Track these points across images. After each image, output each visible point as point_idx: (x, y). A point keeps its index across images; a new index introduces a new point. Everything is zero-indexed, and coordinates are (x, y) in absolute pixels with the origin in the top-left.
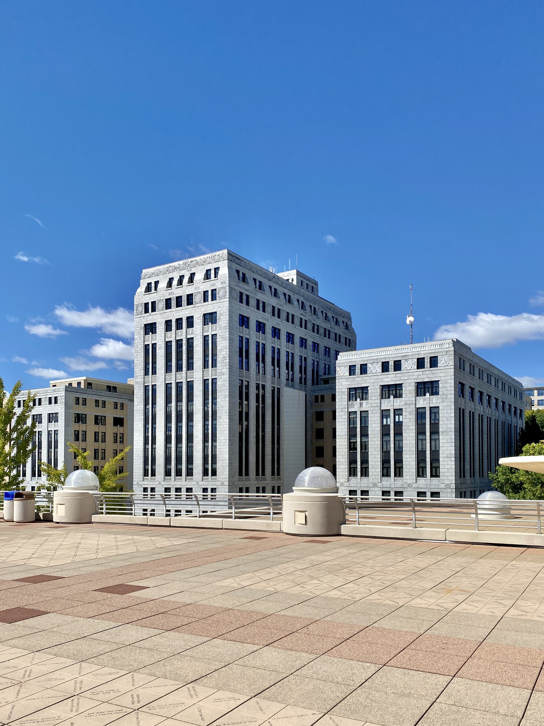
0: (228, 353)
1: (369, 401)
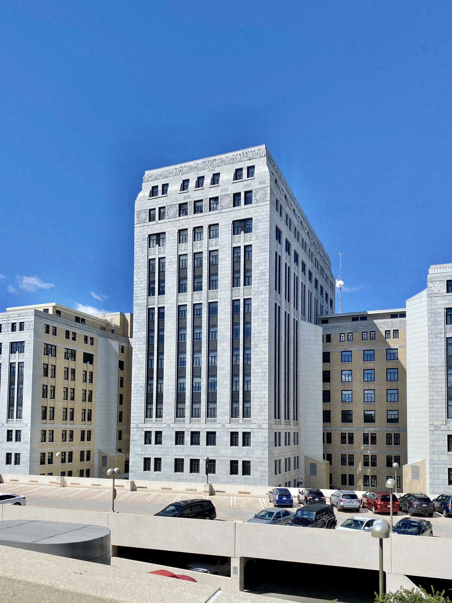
0: (268, 267)
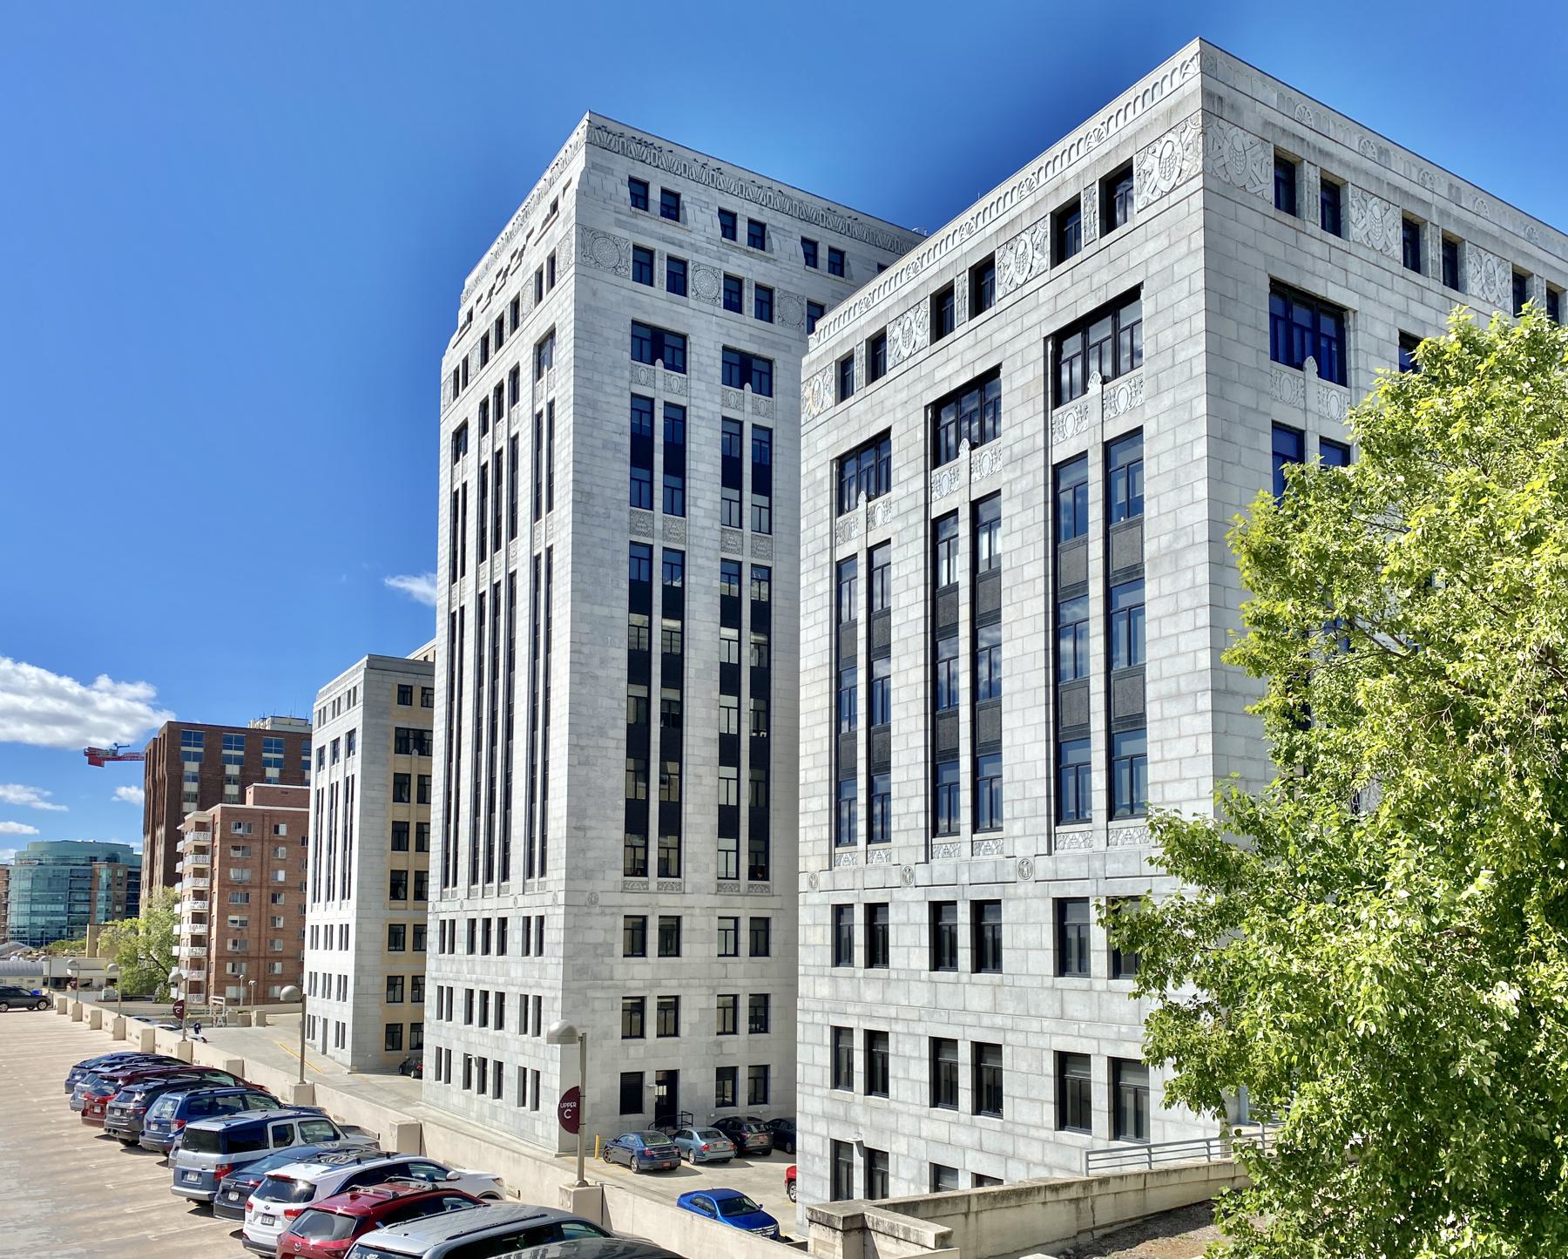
1: (896, 492)
